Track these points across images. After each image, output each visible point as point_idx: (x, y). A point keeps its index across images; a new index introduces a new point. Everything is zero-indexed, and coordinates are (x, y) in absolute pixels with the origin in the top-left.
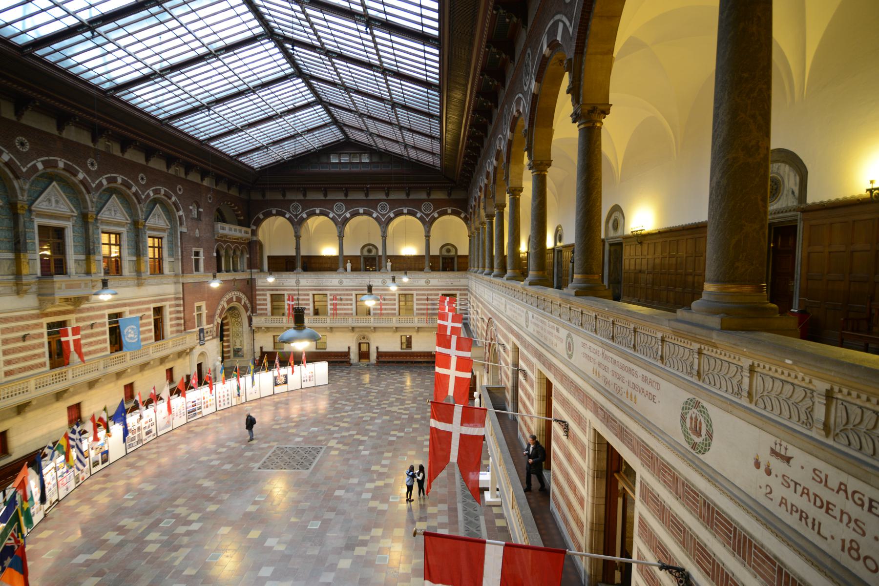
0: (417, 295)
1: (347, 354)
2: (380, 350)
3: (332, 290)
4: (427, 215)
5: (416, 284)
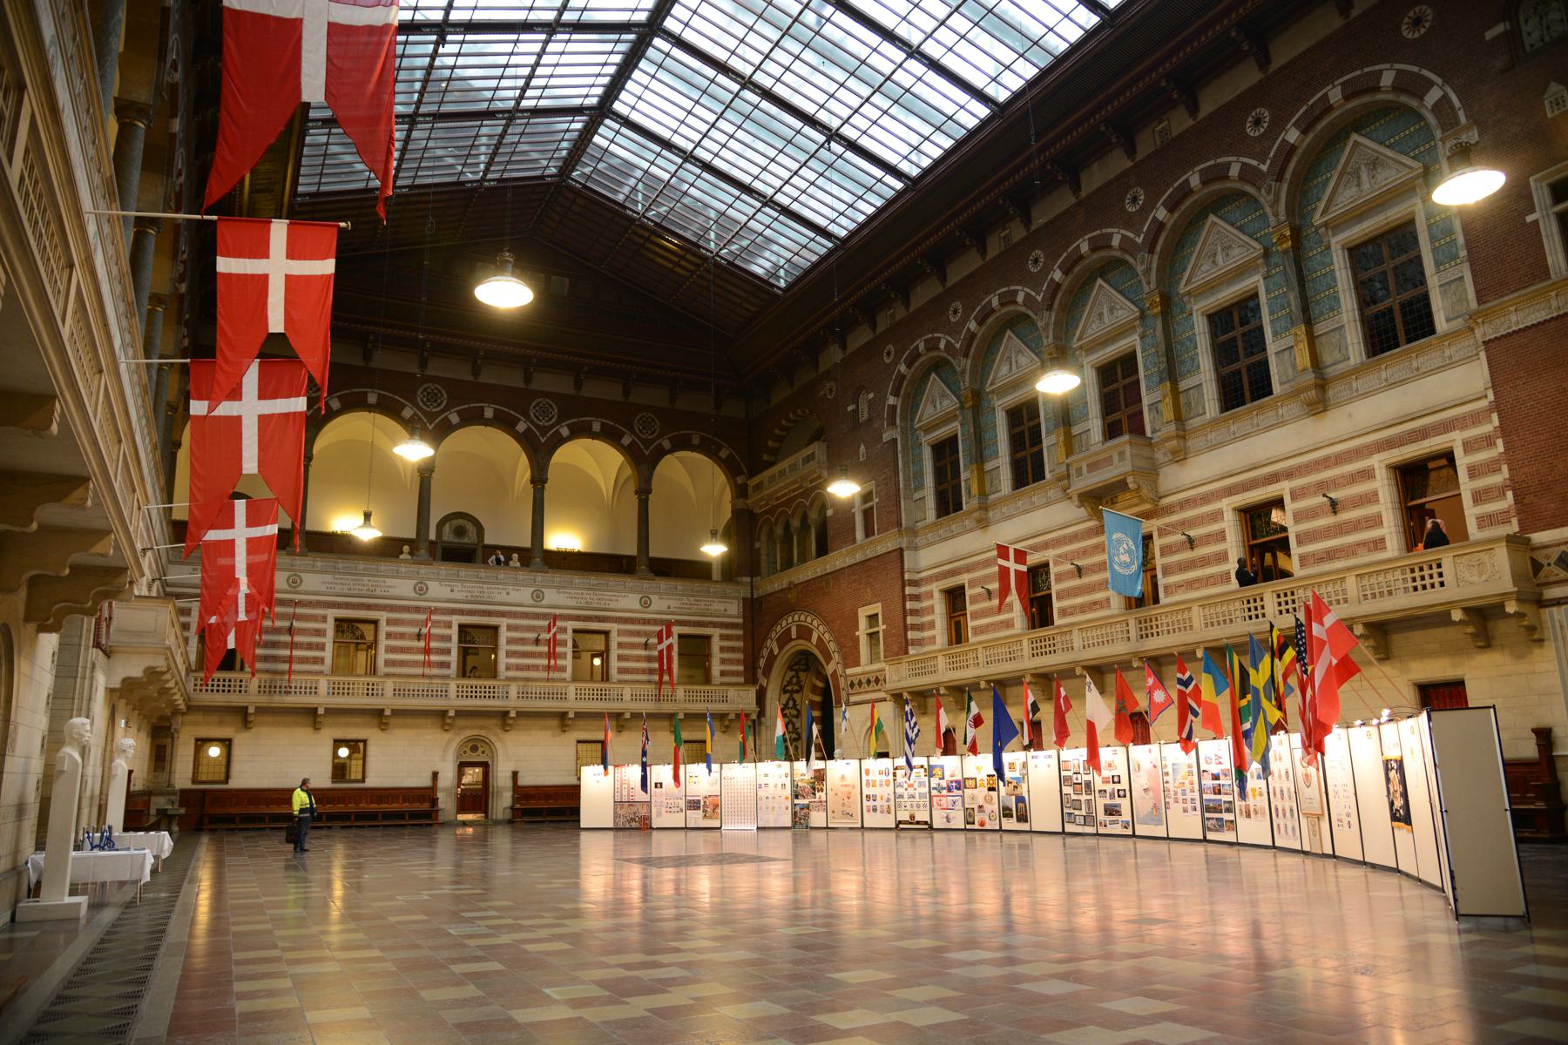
0: (620, 633)
1: (428, 795)
2: (522, 781)
3: (392, 608)
4: (647, 443)
5: (612, 605)
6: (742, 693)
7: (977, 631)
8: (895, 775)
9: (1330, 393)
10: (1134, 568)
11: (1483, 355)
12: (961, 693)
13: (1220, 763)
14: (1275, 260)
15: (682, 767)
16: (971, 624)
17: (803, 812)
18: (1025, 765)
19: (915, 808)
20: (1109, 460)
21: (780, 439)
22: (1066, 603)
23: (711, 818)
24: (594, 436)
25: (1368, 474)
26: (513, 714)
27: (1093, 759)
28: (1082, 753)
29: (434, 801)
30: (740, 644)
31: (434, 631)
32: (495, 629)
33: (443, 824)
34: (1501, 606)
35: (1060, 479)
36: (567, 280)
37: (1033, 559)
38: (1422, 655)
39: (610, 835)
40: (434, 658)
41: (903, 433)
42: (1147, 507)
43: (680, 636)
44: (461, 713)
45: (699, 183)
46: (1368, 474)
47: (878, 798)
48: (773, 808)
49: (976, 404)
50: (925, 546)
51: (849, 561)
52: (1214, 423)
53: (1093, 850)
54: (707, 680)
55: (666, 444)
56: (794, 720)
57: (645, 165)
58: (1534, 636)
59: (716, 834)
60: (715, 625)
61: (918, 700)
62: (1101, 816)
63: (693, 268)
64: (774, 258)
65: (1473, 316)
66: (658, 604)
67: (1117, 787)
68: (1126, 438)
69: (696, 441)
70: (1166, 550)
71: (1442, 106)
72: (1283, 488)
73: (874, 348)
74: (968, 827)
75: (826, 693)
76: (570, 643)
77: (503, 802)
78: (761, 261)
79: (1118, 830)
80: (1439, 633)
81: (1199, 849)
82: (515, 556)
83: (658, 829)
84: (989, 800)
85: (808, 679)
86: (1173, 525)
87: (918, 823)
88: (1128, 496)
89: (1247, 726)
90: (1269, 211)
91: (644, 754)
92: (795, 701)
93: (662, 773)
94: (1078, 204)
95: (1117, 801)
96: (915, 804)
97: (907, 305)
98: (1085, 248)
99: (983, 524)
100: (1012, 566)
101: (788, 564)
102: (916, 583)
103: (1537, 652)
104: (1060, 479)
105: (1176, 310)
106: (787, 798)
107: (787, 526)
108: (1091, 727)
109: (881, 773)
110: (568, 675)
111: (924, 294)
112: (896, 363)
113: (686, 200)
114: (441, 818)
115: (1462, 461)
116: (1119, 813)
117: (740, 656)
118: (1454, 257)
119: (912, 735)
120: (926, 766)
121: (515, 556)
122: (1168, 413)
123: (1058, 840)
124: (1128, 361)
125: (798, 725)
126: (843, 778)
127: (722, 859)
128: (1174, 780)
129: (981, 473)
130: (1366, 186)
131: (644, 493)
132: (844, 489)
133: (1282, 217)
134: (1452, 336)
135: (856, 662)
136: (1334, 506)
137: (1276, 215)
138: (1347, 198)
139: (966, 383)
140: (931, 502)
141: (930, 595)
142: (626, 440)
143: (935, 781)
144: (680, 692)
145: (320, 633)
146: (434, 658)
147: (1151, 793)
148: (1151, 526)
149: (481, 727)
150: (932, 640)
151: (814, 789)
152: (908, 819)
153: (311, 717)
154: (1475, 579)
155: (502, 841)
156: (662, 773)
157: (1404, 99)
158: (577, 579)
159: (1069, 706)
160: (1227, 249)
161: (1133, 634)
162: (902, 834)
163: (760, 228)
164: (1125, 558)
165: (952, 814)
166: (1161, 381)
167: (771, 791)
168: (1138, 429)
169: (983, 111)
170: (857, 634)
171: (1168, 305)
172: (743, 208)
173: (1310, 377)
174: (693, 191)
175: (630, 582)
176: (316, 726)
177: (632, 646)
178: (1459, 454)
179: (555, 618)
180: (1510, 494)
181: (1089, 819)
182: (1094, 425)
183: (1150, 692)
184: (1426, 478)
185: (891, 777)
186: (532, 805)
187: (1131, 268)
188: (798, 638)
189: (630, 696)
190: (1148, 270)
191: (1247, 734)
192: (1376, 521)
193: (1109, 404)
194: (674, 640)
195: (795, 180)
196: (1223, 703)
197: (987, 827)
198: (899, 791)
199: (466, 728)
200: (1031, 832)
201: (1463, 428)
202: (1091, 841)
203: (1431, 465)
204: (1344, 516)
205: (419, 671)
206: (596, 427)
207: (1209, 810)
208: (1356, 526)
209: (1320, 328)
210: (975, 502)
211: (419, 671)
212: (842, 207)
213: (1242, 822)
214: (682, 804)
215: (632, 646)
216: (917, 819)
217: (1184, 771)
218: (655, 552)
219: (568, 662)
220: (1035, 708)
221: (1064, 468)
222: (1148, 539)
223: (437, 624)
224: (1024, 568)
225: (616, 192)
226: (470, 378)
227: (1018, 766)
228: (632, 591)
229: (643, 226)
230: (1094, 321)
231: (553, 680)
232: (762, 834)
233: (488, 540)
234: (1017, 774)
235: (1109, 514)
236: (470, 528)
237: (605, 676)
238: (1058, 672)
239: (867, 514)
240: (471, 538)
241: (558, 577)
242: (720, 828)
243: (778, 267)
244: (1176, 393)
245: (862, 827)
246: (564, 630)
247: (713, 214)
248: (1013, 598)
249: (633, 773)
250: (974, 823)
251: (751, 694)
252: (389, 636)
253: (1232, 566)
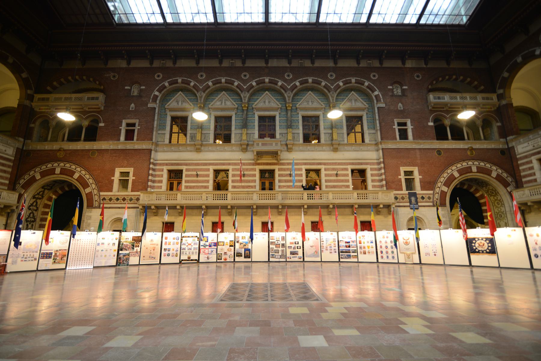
6: (10, 195)
8: (182, 240)
13: (350, 238)
17: (125, 258)
19: (191, 254)
21: (61, 84)
23: (59, 263)
25: (346, 169)
30: (10, 170)
47: (171, 250)
48: (106, 256)
50: (161, 152)
52: (301, 144)
56: (34, 212)
59: (62, 272)
62: (288, 255)
67: (297, 245)
74: (218, 261)
79: (296, 259)
83: (11, 272)
87: (192, 260)
92: (37, 203)
96: (191, 252)
102: (154, 164)
106: (115, 250)
109: (174, 239)
116: (297, 254)
117: (8, 176)
120: (198, 236)
125: (35, 214)
126: (152, 240)
128: (326, 243)
133: (202, 101)
138: (305, 105)
147: (314, 247)
150: (160, 187)
151: (133, 246)
152: (187, 259)
154: (386, 198)
160: (312, 102)
162: (183, 265)
165: (210, 256)
167: (105, 247)
169: (212, 20)
170: (421, 177)
178: (184, 171)
181: (284, 256)
185: (180, 241)
192: (208, 181)
197: (228, 260)
200: (252, 262)
202: (284, 264)
204: (339, 178)
208: (342, 181)
214: (37, 255)
216: (191, 258)
230: (261, 103)
232: (96, 270)
242: (65, 269)
245: (160, 263)
250: (221, 259)
251: (15, 196)
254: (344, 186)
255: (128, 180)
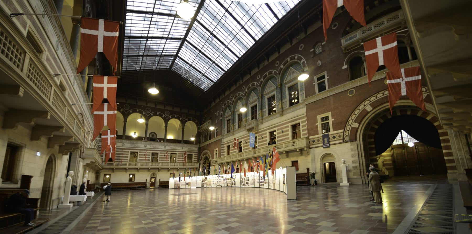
0: (178, 154)
1: (145, 184)
2: (161, 181)
5: (177, 149)
7: (232, 153)
9: (284, 113)
10: (253, 142)
11: (305, 107)
12: (228, 163)
14: (278, 89)
15: (185, 177)
16: (231, 152)
18: (236, 176)
20: (251, 124)
22: (244, 148)
24: (175, 118)
26: (160, 169)
27: (245, 175)
28: (244, 173)
29: (146, 185)
31: (147, 154)
32: (158, 153)
33: (147, 189)
34: (304, 149)
35: (244, 127)
36: (171, 89)
37: (240, 141)
38: (293, 157)
39: (174, 190)
40: (147, 159)
41: (223, 118)
42: (256, 132)
43: (188, 154)
44: (151, 169)
45: (193, 71)
46: (288, 127)
49: (233, 113)
51: (214, 141)
52: (267, 117)
53: (244, 190)
54: (192, 162)
55: (187, 120)
57: (184, 67)
58: (308, 153)
60: (193, 152)
61: (222, 165)
63: (191, 87)
64: (205, 86)
65: (304, 100)
66: (185, 149)
68: (254, 120)
69: (192, 119)
70: (259, 139)
71: (304, 63)
72: (276, 129)
73: (220, 102)
75: (209, 164)
76: (170, 156)
77: (158, 184)
78: (203, 86)
80: (295, 153)
81: (258, 189)
82: (162, 140)
84: (230, 182)
85: (207, 161)
86: (260, 135)
88: (254, 130)
89: (265, 169)
90: (278, 80)
91: (180, 175)
93: (182, 178)
94: (251, 77)
95: (248, 181)
97: (224, 95)
98: (251, 85)
99: (233, 134)
100: (236, 142)
101: (205, 141)
103: (308, 156)
104: (244, 127)
105: (263, 97)
107: (205, 135)
108: (245, 169)
110: (169, 161)
111: (227, 93)
112: (222, 105)
113: (191, 74)
114: (147, 188)
115: (301, 125)
118: (303, 90)
119: (220, 171)
121: (162, 140)
122: (261, 115)
123: (239, 188)
124: (256, 106)
127: (190, 194)
129: (234, 125)
130: (292, 76)
131: (183, 128)
132: (212, 128)
134: (302, 103)
135: (214, 159)
136: (283, 132)
137: (279, 81)
139: (232, 109)
140: (226, 131)
141: (225, 147)
142: (181, 119)
143: (223, 179)
144: (187, 164)
145: (127, 154)
146: (147, 159)
148: (257, 135)
149: (155, 171)
153: (125, 170)
155: (157, 192)
156: (182, 178)
157: (298, 61)
158: (172, 144)
159: (242, 166)
161: (253, 153)
163: (202, 80)
164: (252, 140)
166: (260, 110)
168: (256, 118)
171: (262, 96)
172: (200, 76)
173: (281, 110)
174: (192, 72)
175: (180, 145)
176: (126, 172)
177: (180, 156)
179: (168, 151)
180: (307, 130)
182: (250, 117)
183: (253, 163)
184: (296, 127)
186: (163, 185)
187: (257, 89)
188: (206, 154)
189: (179, 165)
190: (260, 90)
191: (265, 170)
193: (253, 114)
194: (187, 155)
195: (208, 71)
196: (263, 165)
198: (218, 180)
199: (152, 171)
201: (302, 119)
203: (297, 125)
205: (144, 161)
206: (176, 116)
207: (260, 182)
209: (283, 101)
210: (232, 131)
211: (144, 161)
212: (215, 76)
213: (265, 185)
214: (185, 184)
215: (180, 156)
217: (257, 176)
218: (184, 139)
219: (169, 159)
220: (237, 166)
221: (245, 125)
222: (256, 137)
223: (148, 153)
224: (238, 142)
225: (179, 72)
226: (155, 107)
227: (235, 176)
228: (181, 146)
229: (184, 79)
231: (167, 162)
233: (158, 137)
234: (234, 177)
235: (251, 133)
236: (155, 135)
237: (175, 162)
238: (249, 159)
239: (217, 132)
240: (155, 137)
241: (169, 144)
243: (205, 87)
244: (262, 112)
246: (169, 153)
247: (195, 77)
248: (236, 147)
249: (178, 179)
252: (140, 155)
253: (268, 142)
254: (286, 138)
255: (329, 122)
